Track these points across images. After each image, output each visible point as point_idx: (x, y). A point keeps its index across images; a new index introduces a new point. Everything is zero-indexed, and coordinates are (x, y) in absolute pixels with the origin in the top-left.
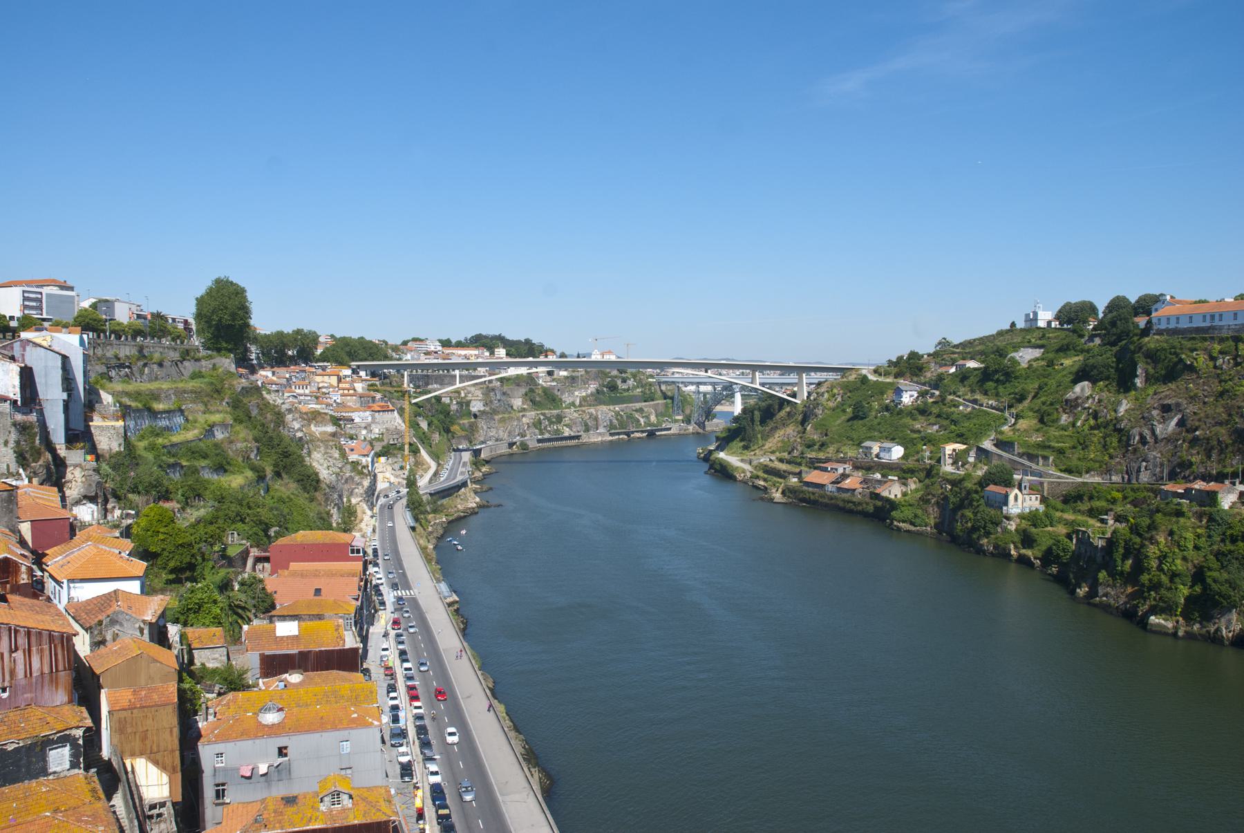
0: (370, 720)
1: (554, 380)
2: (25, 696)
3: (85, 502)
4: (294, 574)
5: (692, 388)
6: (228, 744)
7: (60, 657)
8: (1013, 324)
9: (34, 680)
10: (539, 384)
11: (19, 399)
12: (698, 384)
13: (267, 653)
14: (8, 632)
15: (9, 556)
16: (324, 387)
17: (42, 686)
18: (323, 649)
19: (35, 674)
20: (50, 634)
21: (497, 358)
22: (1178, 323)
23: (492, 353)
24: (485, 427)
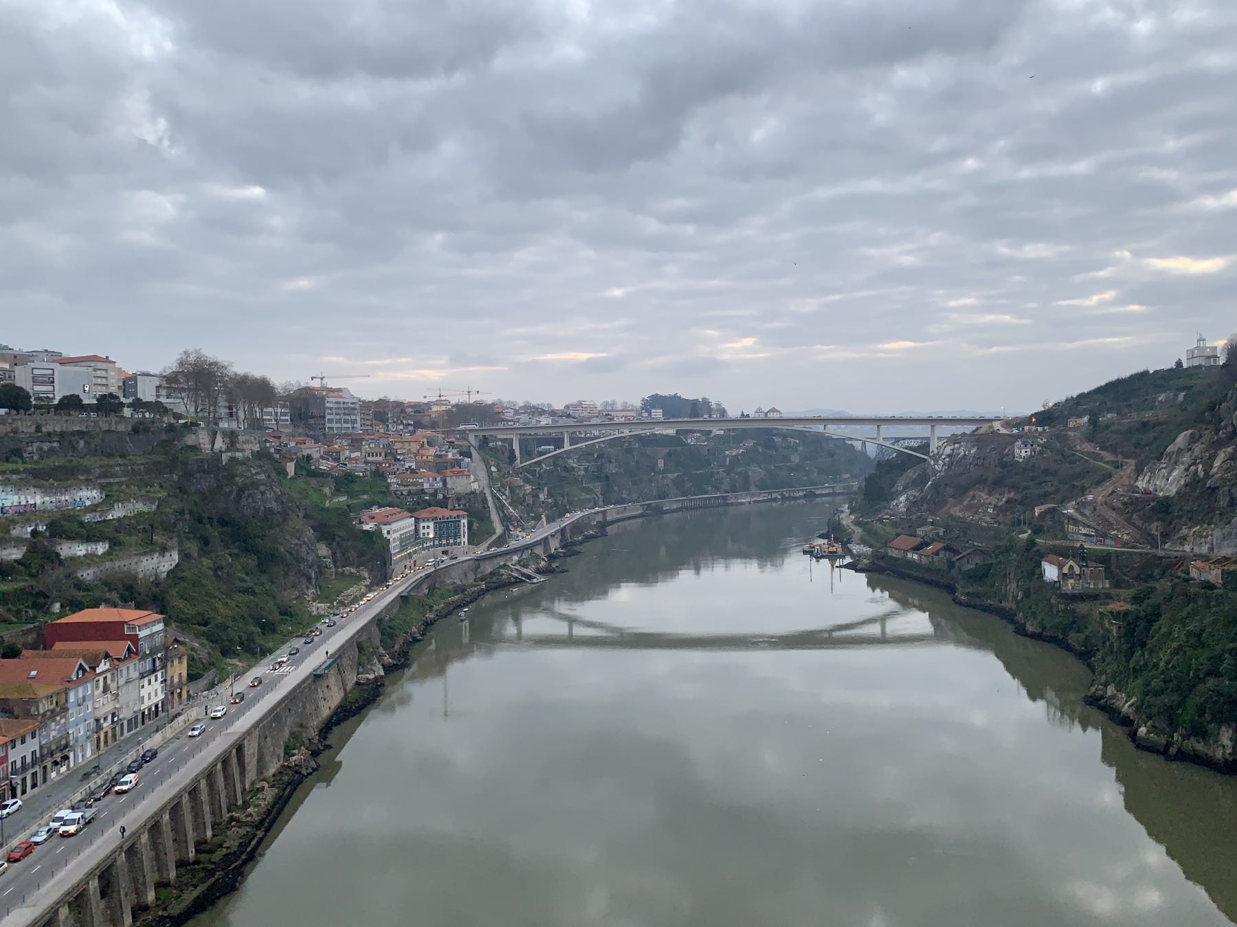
10: (686, 444)
23: (650, 414)
24: (616, 489)
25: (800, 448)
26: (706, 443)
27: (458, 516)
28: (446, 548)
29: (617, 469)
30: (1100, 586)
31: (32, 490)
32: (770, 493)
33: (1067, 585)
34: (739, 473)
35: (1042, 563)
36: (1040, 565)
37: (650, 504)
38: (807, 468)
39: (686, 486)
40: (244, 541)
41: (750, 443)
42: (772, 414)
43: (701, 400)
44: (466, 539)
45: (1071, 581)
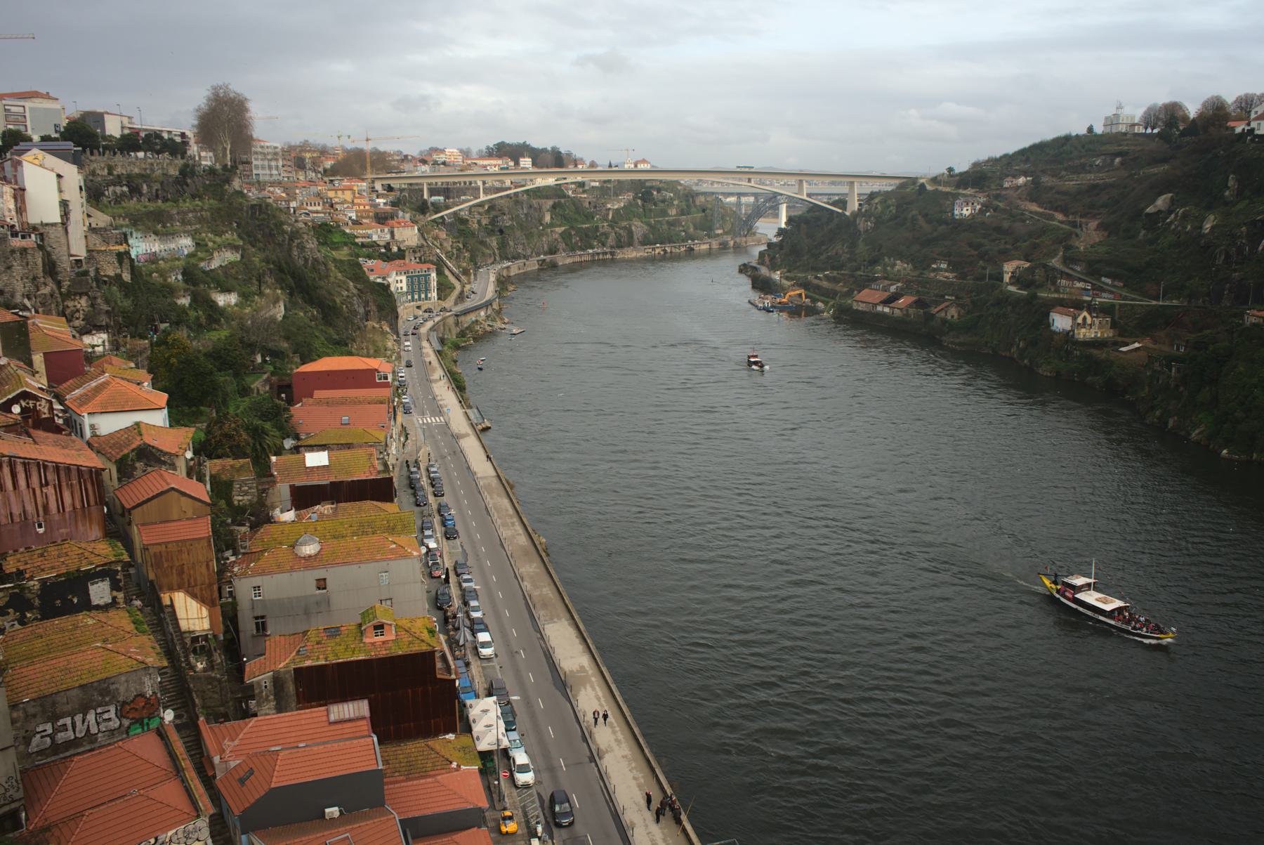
0: (409, 551)
1: (584, 192)
2: (61, 531)
3: (94, 332)
4: (319, 402)
5: (732, 199)
6: (264, 577)
8: (1090, 129)
9: (67, 515)
10: (569, 197)
11: (17, 224)
12: (739, 195)
13: (298, 484)
15: (28, 390)
16: (337, 203)
18: (355, 479)
19: (67, 510)
20: (78, 469)
21: (523, 168)
23: (517, 163)
24: (511, 243)
25: (676, 202)
26: (585, 196)
27: (428, 269)
28: (419, 303)
29: (510, 222)
30: (1106, 335)
31: (153, 237)
33: (1079, 334)
34: (625, 228)
35: (1051, 314)
36: (1048, 315)
39: (573, 241)
40: (308, 294)
41: (630, 196)
45: (1083, 330)
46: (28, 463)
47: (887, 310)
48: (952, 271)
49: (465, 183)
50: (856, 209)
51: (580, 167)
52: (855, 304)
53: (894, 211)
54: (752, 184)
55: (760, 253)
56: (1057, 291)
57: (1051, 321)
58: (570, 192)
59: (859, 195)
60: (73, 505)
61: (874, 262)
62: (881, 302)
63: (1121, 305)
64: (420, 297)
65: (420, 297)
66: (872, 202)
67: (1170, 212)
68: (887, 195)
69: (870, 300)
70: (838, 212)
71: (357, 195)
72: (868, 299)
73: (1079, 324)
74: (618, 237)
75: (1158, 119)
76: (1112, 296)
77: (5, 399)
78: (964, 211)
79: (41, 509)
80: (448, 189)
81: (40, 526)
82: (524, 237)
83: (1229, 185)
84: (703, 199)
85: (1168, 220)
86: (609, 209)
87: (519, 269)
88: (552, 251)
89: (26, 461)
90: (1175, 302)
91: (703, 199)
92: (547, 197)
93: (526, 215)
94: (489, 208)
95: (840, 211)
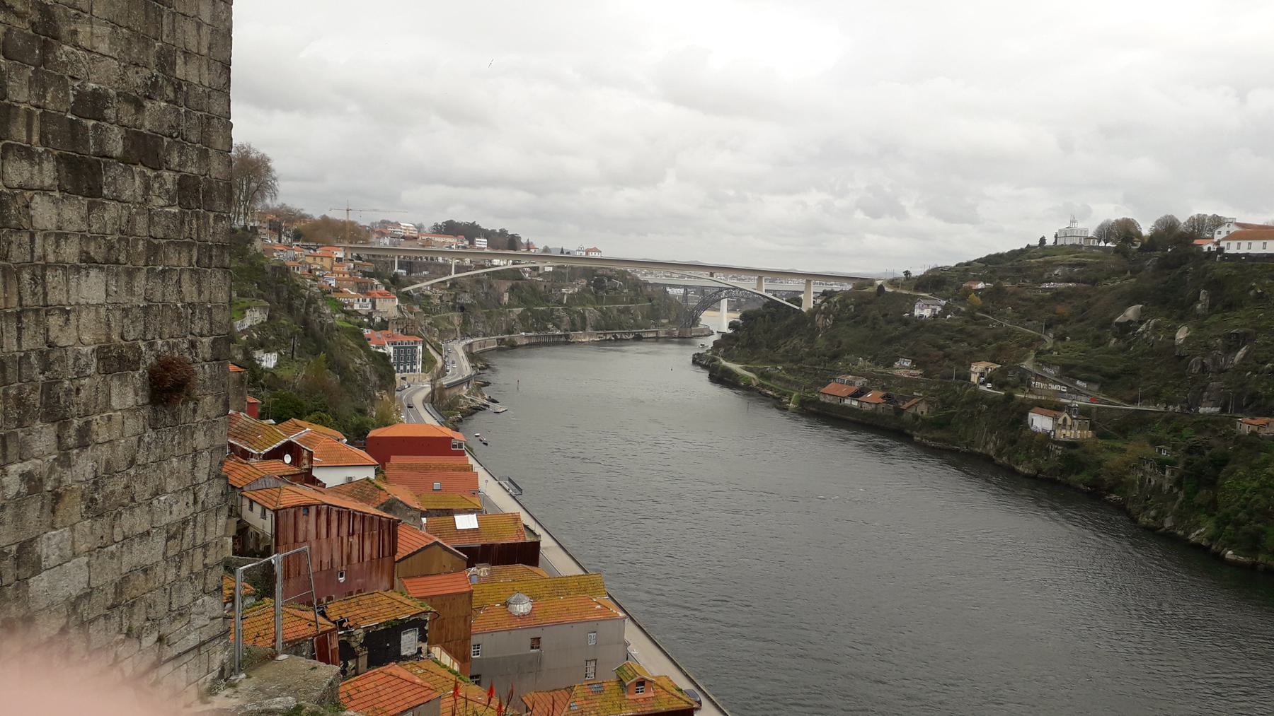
1: (539, 275)
5: (682, 291)
7: (386, 543)
8: (1043, 240)
9: (365, 565)
10: (526, 280)
12: (686, 287)
14: (347, 517)
16: (316, 269)
17: (371, 573)
19: (366, 560)
20: (380, 519)
21: (479, 248)
22: (1249, 248)
23: (472, 243)
24: (472, 321)
32: (605, 334)
34: (578, 312)
35: (1030, 414)
37: (503, 339)
38: (632, 312)
41: (584, 282)
42: (593, 253)
43: (498, 231)
44: (419, 367)
46: (342, 511)
47: (855, 403)
48: (916, 369)
49: (427, 258)
50: (812, 307)
51: (533, 251)
52: (821, 396)
53: (853, 310)
54: (714, 278)
55: (714, 342)
56: (1031, 392)
57: (1030, 422)
58: (527, 275)
59: (814, 293)
60: (371, 555)
61: (835, 357)
62: (850, 396)
63: (1098, 408)
64: (405, 368)
65: (405, 368)
66: (831, 300)
67: (1141, 323)
68: (845, 295)
69: (837, 393)
70: (794, 309)
71: (335, 263)
72: (838, 390)
73: (1059, 425)
74: (573, 323)
75: (1109, 233)
76: (1088, 399)
77: (270, 448)
78: (924, 311)
79: (345, 558)
80: (411, 263)
81: (341, 576)
82: (484, 316)
83: (1200, 299)
84: (650, 290)
85: (1140, 330)
86: (564, 294)
87: (480, 347)
88: (510, 331)
89: (341, 509)
90: (1152, 408)
91: (650, 290)
92: (505, 278)
93: (486, 294)
94: (451, 284)
95: (798, 308)
